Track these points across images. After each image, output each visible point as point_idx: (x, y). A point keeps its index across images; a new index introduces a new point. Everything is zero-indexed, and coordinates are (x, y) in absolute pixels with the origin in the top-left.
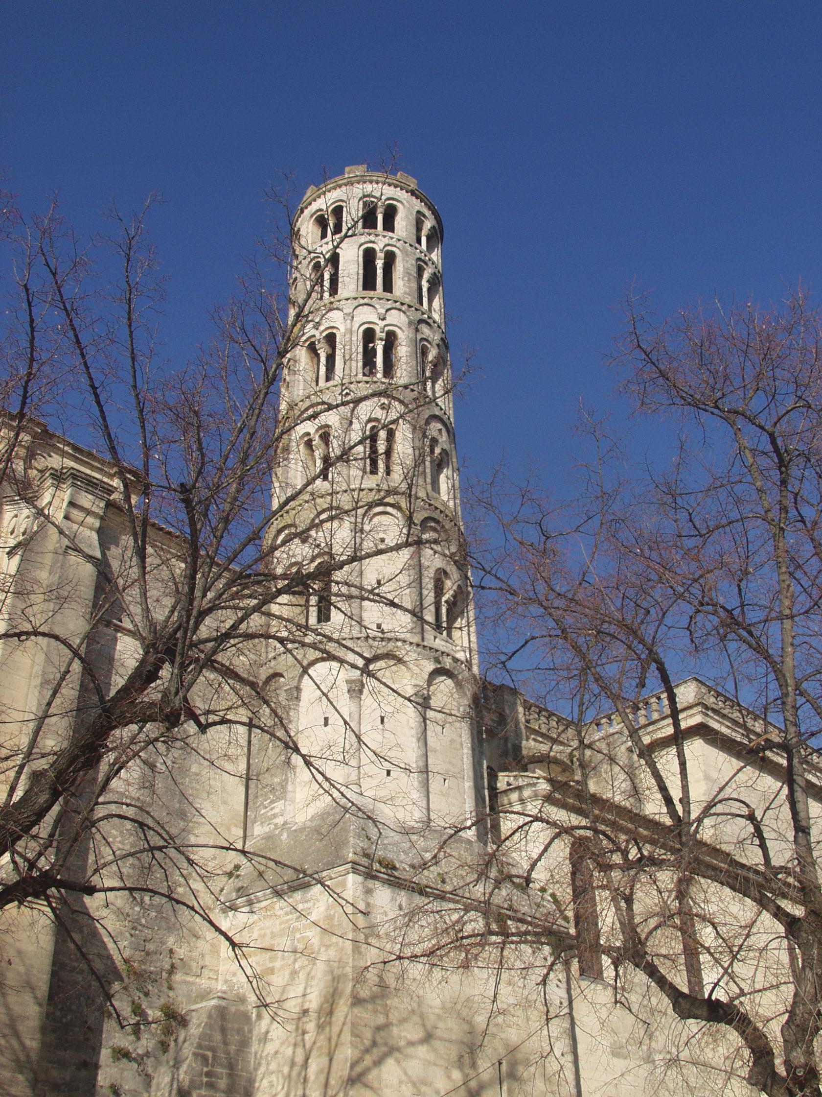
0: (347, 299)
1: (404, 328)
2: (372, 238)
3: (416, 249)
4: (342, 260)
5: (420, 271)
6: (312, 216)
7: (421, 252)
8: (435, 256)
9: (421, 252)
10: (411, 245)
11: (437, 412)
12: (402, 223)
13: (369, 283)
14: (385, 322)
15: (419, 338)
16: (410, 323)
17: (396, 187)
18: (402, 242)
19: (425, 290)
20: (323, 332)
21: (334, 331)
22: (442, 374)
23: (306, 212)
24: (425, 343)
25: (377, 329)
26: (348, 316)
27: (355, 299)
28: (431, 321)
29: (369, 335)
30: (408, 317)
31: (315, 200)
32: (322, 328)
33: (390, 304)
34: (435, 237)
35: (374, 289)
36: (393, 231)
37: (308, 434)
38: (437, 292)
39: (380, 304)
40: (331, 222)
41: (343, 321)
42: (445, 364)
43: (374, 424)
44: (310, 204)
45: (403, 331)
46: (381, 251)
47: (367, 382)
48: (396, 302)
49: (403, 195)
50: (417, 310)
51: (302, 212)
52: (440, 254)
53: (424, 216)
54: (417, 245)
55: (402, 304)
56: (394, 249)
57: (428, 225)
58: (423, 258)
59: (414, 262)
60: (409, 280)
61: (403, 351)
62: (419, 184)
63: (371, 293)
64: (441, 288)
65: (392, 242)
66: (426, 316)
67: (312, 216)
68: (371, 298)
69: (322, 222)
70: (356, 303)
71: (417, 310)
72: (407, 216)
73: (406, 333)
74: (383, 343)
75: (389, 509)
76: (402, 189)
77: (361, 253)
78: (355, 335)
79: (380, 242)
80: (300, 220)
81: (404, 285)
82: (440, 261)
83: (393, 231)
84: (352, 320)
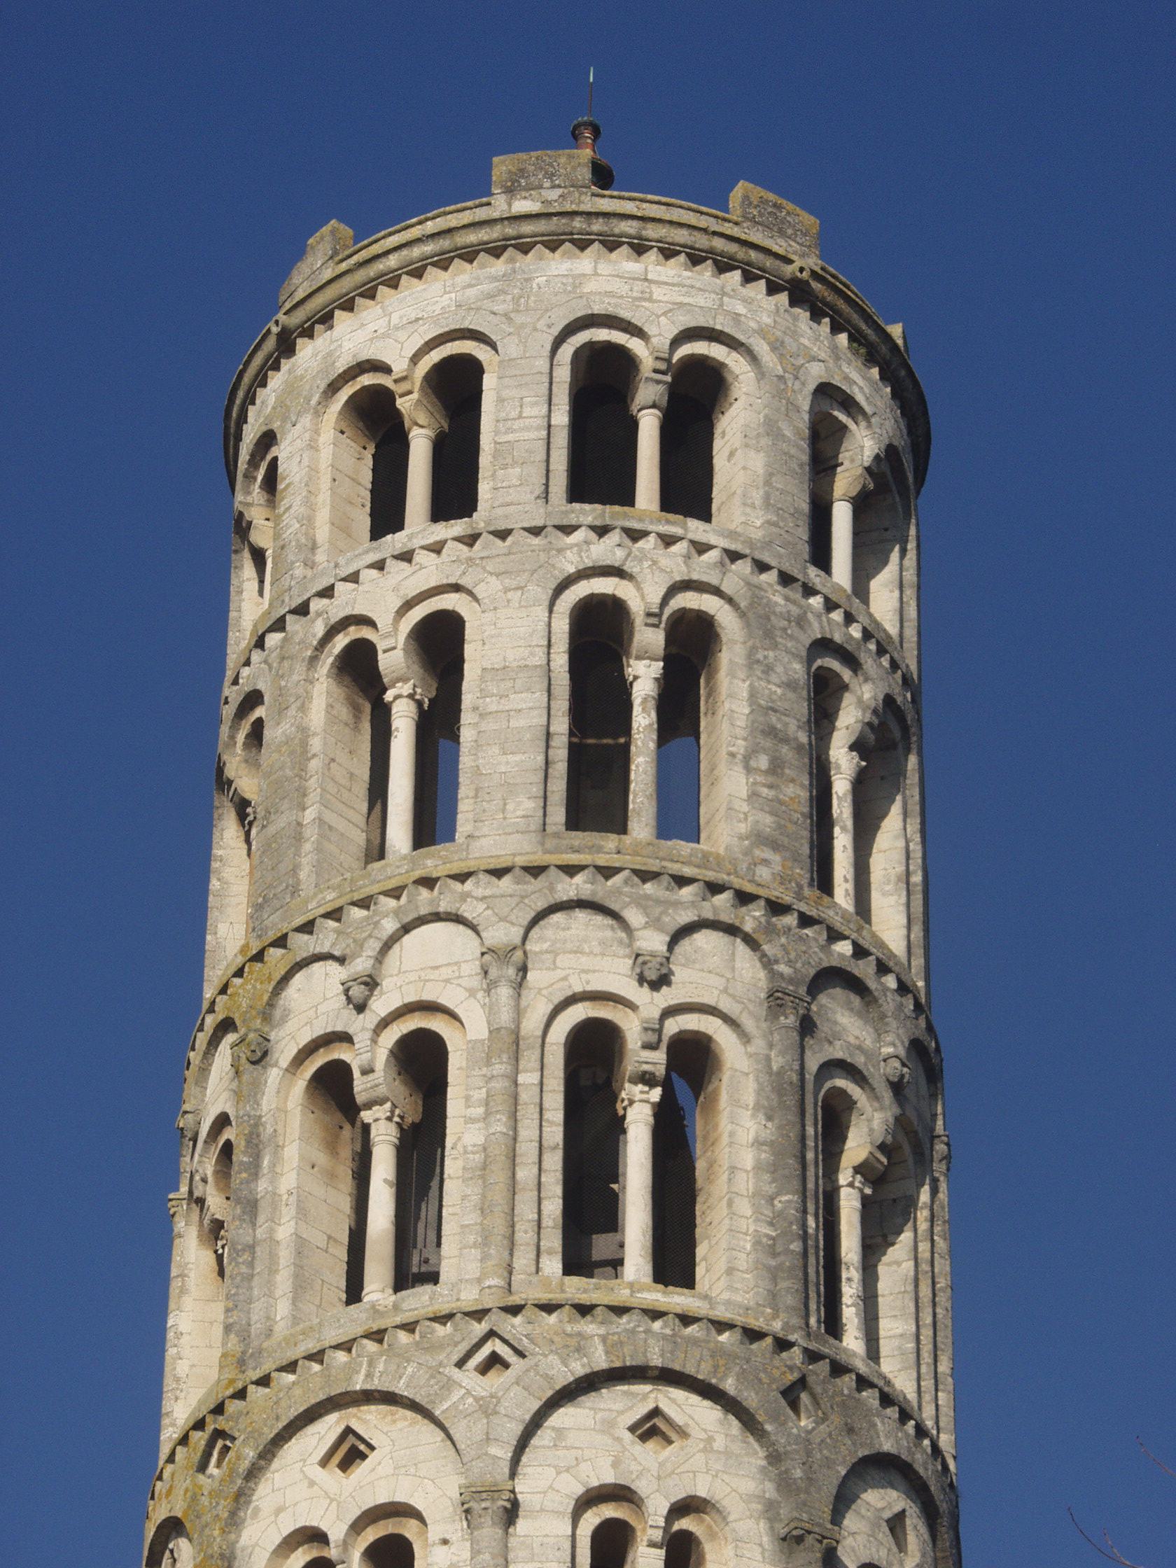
0: (499, 873)
1: (748, 1023)
2: (607, 550)
3: (809, 591)
4: (476, 657)
5: (824, 696)
6: (333, 388)
7: (830, 605)
8: (887, 600)
9: (830, 605)
10: (786, 579)
11: (888, 1437)
12: (748, 454)
13: (593, 790)
14: (667, 997)
15: (813, 1065)
16: (776, 1000)
17: (723, 266)
18: (744, 567)
19: (841, 786)
20: (384, 1023)
21: (436, 1024)
22: (910, 1204)
23: (308, 354)
24: (841, 1083)
25: (632, 1029)
26: (494, 962)
27: (535, 871)
28: (864, 970)
29: (593, 1052)
30: (767, 963)
31: (349, 306)
32: (381, 1005)
34: (888, 502)
35: (619, 825)
36: (706, 516)
37: (316, 1536)
38: (895, 780)
39: (642, 903)
40: (422, 442)
41: (476, 982)
42: (922, 1157)
43: (610, 1511)
44: (326, 319)
45: (745, 1037)
46: (653, 617)
47: (584, 1310)
48: (714, 888)
49: (752, 309)
50: (806, 921)
51: (286, 346)
52: (910, 576)
53: (849, 404)
54: (813, 574)
55: (744, 898)
57: (862, 446)
58: (838, 638)
59: (798, 669)
60: (776, 767)
61: (740, 1136)
62: (826, 244)
63: (606, 848)
64: (913, 761)
65: (705, 567)
66: (844, 948)
67: (333, 388)
68: (607, 872)
69: (376, 417)
70: (538, 894)
71: (806, 921)
72: (771, 429)
73: (758, 1045)
74: (656, 1094)
76: (748, 278)
77: (562, 625)
78: (530, 1059)
79: (650, 571)
80: (276, 381)
81: (753, 796)
82: (911, 633)
83: (706, 516)
84: (519, 985)
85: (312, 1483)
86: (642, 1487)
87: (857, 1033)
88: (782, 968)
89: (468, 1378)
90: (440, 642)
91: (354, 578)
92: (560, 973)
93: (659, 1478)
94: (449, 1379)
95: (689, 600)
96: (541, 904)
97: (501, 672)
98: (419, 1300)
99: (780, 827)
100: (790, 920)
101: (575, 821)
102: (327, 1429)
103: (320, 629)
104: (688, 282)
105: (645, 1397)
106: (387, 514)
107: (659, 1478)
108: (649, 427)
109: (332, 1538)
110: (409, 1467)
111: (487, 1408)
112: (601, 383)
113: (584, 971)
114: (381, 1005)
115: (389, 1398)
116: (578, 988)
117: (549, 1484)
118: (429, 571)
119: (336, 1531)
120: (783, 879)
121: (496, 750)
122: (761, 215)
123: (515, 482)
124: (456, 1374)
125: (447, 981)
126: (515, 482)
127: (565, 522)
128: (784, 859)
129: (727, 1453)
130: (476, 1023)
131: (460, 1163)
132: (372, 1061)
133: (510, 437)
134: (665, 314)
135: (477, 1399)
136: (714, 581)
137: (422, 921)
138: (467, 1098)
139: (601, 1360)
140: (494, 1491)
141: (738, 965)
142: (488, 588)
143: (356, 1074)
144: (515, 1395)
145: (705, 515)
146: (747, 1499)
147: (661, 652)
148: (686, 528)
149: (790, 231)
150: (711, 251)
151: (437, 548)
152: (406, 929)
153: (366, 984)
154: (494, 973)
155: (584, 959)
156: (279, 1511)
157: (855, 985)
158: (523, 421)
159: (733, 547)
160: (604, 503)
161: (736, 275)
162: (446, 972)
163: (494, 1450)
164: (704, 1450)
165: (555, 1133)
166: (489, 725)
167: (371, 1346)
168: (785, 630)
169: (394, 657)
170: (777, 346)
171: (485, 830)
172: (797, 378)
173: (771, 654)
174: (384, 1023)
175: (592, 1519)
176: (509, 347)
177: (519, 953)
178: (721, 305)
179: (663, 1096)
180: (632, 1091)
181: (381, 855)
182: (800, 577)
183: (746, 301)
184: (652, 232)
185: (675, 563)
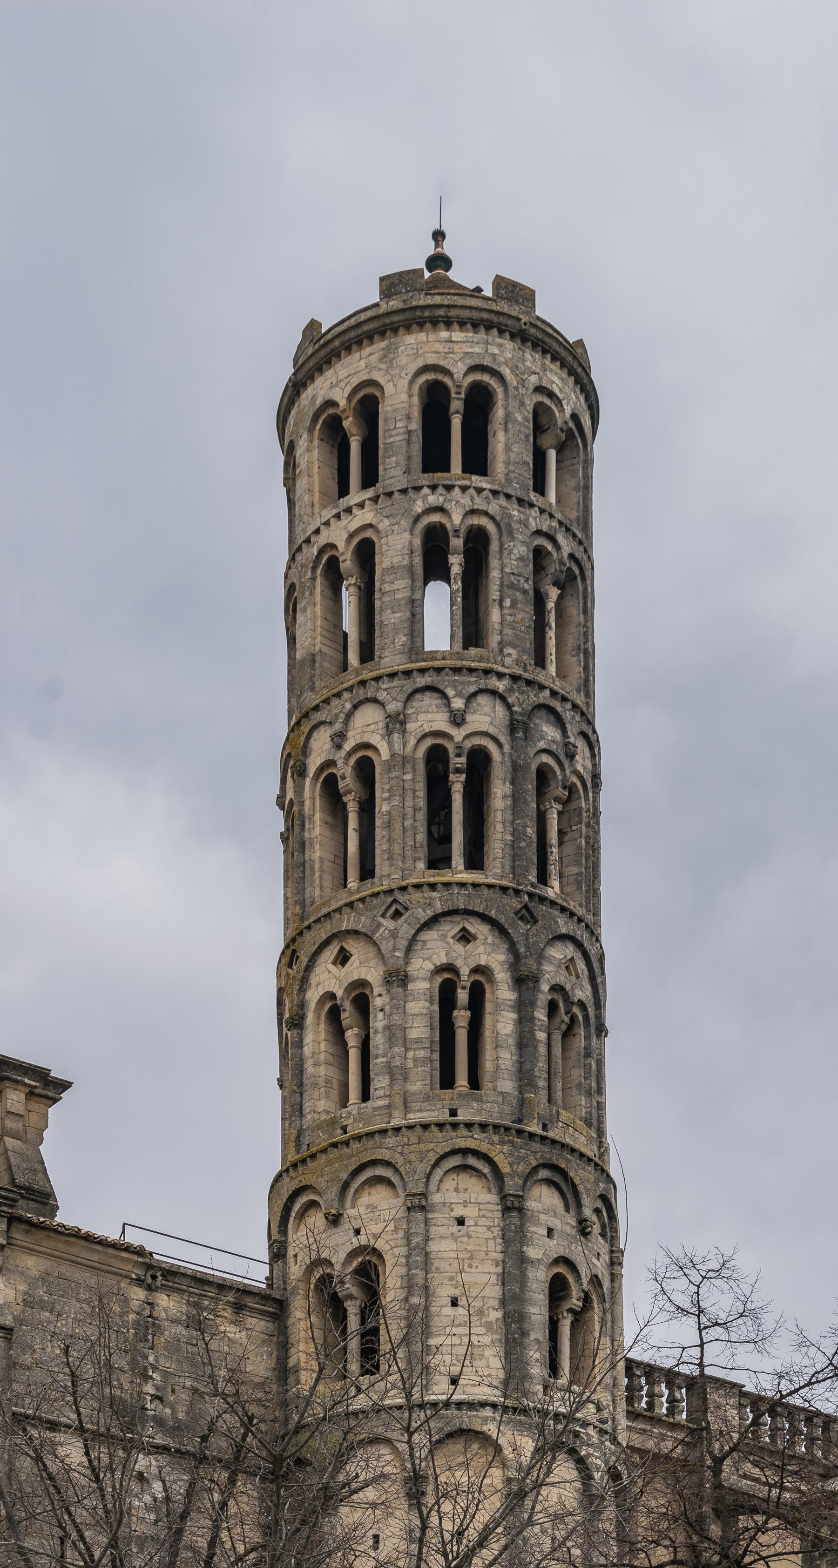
1: (503, 739)
10: (520, 501)
17: (489, 327)
21: (370, 753)
27: (408, 673)
29: (436, 758)
30: (509, 707)
32: (348, 746)
33: (473, 684)
43: (446, 976)
45: (500, 745)
56: (484, 521)
70: (409, 686)
74: (463, 777)
75: (472, 1161)
85: (329, 972)
86: (459, 963)
87: (552, 734)
88: (516, 709)
89: (388, 924)
90: (366, 552)
91: (327, 524)
92: (419, 723)
93: (465, 959)
94: (379, 922)
95: (476, 521)
96: (410, 690)
97: (392, 569)
99: (516, 635)
100: (522, 684)
103: (315, 551)
104: (470, 339)
105: (459, 923)
107: (465, 959)
108: (456, 422)
109: (338, 996)
111: (394, 934)
112: (434, 399)
113: (430, 721)
114: (348, 746)
115: (356, 933)
116: (427, 730)
117: (421, 966)
119: (339, 993)
120: (518, 662)
121: (389, 611)
122: (506, 293)
123: (394, 465)
124: (382, 920)
125: (373, 732)
126: (394, 465)
127: (416, 485)
128: (518, 652)
129: (493, 944)
130: (385, 754)
131: (381, 820)
133: (391, 440)
134: (460, 360)
135: (390, 931)
136: (485, 508)
137: (361, 702)
138: (383, 789)
139: (439, 907)
140: (398, 972)
141: (497, 709)
143: (339, 779)
144: (405, 928)
146: (502, 963)
147: (462, 549)
148: (472, 482)
149: (521, 300)
150: (482, 320)
151: (361, 505)
152: (355, 707)
153: (339, 736)
154: (391, 726)
155: (429, 715)
156: (318, 984)
157: (551, 710)
159: (493, 488)
160: (433, 472)
161: (495, 332)
162: (372, 727)
163: (397, 954)
164: (483, 944)
165: (422, 803)
166: (386, 599)
167: (348, 910)
168: (518, 529)
169: (347, 563)
170: (514, 369)
171: (386, 654)
172: (524, 386)
173: (512, 544)
174: (350, 754)
175: (439, 980)
176: (389, 389)
177: (402, 716)
178: (487, 350)
179: (466, 778)
180: (452, 777)
181: (345, 669)
182: (526, 499)
183: (500, 346)
184: (453, 313)
185: (466, 501)
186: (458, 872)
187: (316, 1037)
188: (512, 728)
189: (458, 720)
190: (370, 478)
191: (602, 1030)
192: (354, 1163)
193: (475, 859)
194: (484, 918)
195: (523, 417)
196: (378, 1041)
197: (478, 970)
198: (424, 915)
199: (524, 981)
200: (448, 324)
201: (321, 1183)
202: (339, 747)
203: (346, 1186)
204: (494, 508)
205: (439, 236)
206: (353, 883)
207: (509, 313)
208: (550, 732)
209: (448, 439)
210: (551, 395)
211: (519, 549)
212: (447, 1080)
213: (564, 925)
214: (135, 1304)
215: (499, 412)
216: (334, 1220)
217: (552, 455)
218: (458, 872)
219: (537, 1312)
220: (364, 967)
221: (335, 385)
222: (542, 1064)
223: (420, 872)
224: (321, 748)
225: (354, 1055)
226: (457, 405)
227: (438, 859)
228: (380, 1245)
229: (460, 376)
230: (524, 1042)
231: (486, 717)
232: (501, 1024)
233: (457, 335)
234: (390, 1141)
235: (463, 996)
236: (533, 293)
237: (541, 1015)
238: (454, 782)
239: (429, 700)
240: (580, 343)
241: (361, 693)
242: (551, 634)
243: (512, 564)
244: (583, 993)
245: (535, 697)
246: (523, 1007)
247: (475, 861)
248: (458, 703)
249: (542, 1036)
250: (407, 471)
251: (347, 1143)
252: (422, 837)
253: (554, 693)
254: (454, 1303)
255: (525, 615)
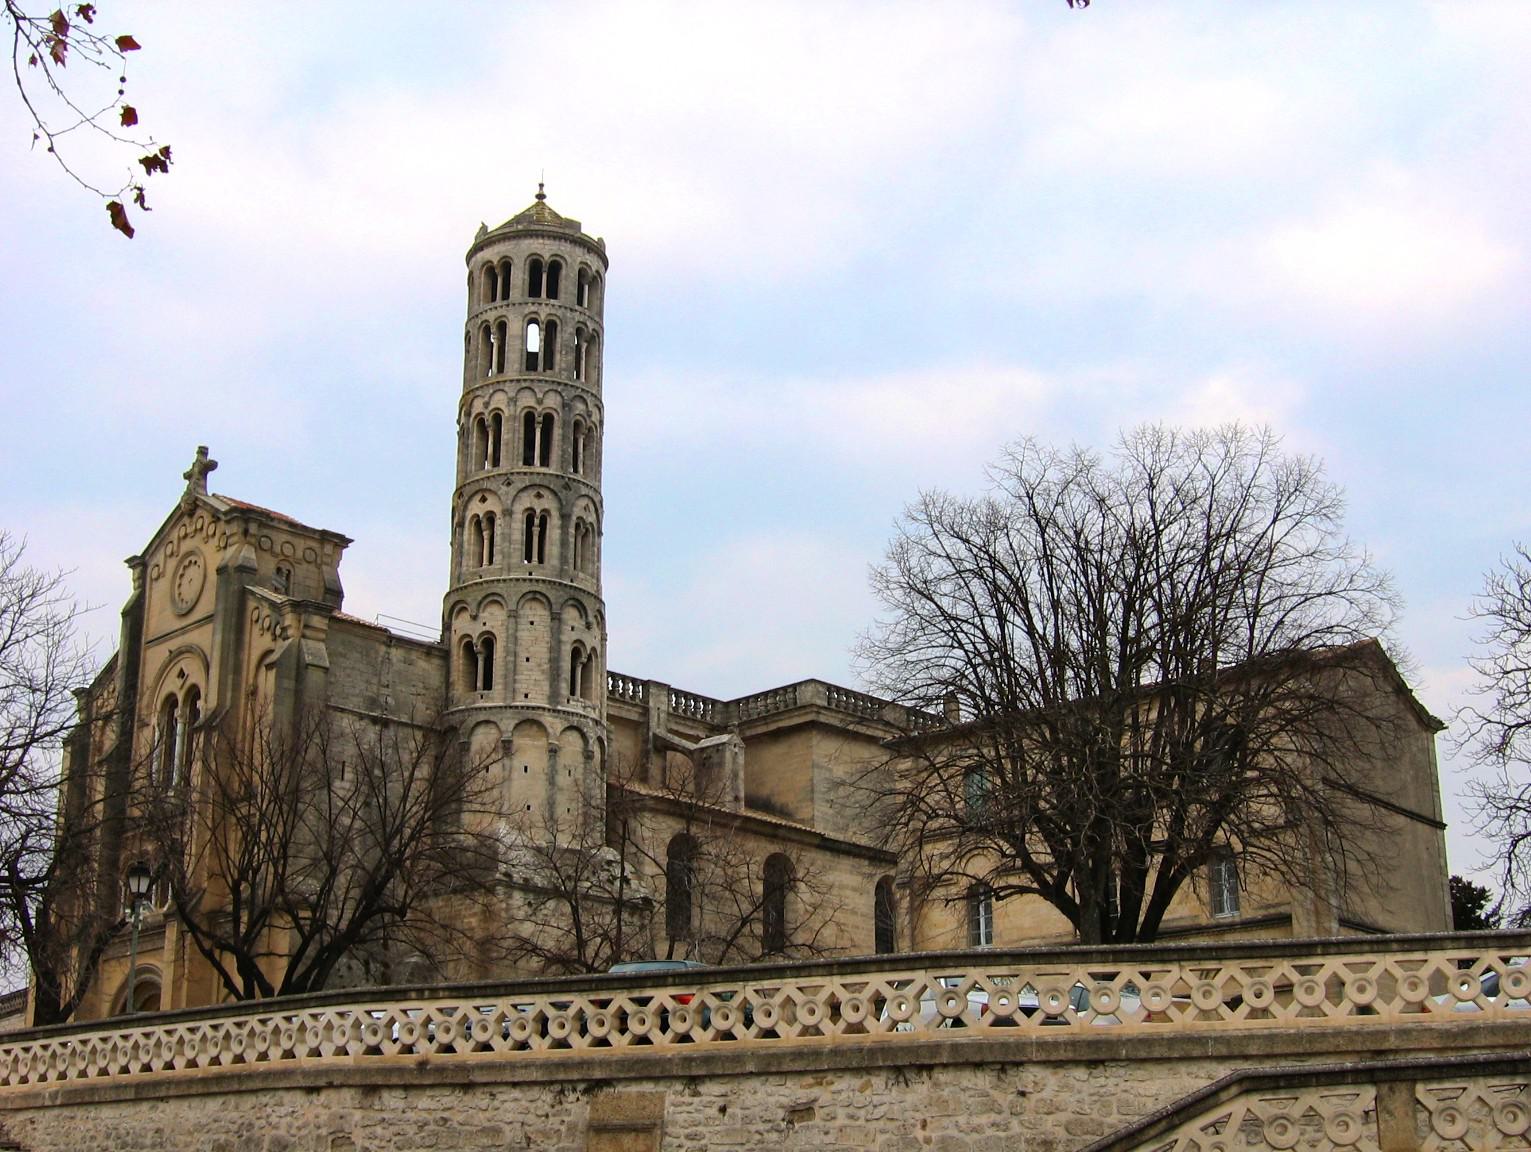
10: (571, 310)
17: (560, 238)
27: (518, 381)
29: (529, 419)
35: (535, 369)
54: (577, 307)
56: (554, 318)
75: (538, 596)
89: (504, 488)
90: (502, 327)
98: (496, 471)
101: (528, 369)
102: (478, 497)
106: (494, 299)
110: (492, 504)
111: (507, 493)
112: (535, 266)
114: (490, 408)
118: (501, 312)
132: (488, 419)
142: (511, 317)
144: (512, 490)
145: (556, 298)
152: (495, 392)
157: (581, 397)
158: (519, 277)
165: (522, 436)
170: (571, 256)
186: (537, 467)
187: (469, 533)
188: (564, 405)
189: (540, 402)
190: (506, 295)
191: (600, 534)
192: (484, 594)
193: (545, 462)
194: (548, 488)
195: (574, 275)
196: (497, 539)
197: (544, 510)
198: (521, 485)
199: (565, 517)
200: (543, 237)
201: (469, 600)
202: (486, 408)
203: (480, 603)
204: (559, 313)
205: (541, 186)
206: (488, 466)
207: (568, 232)
208: (580, 407)
209: (538, 284)
210: (586, 264)
211: (571, 329)
212: (529, 558)
213: (584, 491)
214: (382, 653)
215: (563, 272)
216: (475, 618)
217: (586, 287)
218: (537, 467)
219: (566, 664)
220: (492, 504)
221: (492, 254)
222: (572, 552)
223: (521, 467)
224: (478, 406)
225: (486, 543)
226: (545, 269)
227: (528, 460)
228: (494, 631)
229: (547, 257)
230: (564, 543)
231: (552, 401)
232: (554, 533)
233: (547, 242)
234: (501, 585)
235: (537, 521)
236: (580, 224)
237: (572, 531)
238: (537, 426)
239: (527, 393)
240: (600, 240)
241: (498, 387)
242: (583, 363)
243: (566, 336)
244: (591, 518)
245: (573, 393)
246: (564, 528)
247: (545, 462)
248: (540, 396)
249: (572, 540)
250: (522, 295)
251: (481, 583)
252: (521, 450)
253: (583, 390)
254: (528, 660)
255: (571, 358)
